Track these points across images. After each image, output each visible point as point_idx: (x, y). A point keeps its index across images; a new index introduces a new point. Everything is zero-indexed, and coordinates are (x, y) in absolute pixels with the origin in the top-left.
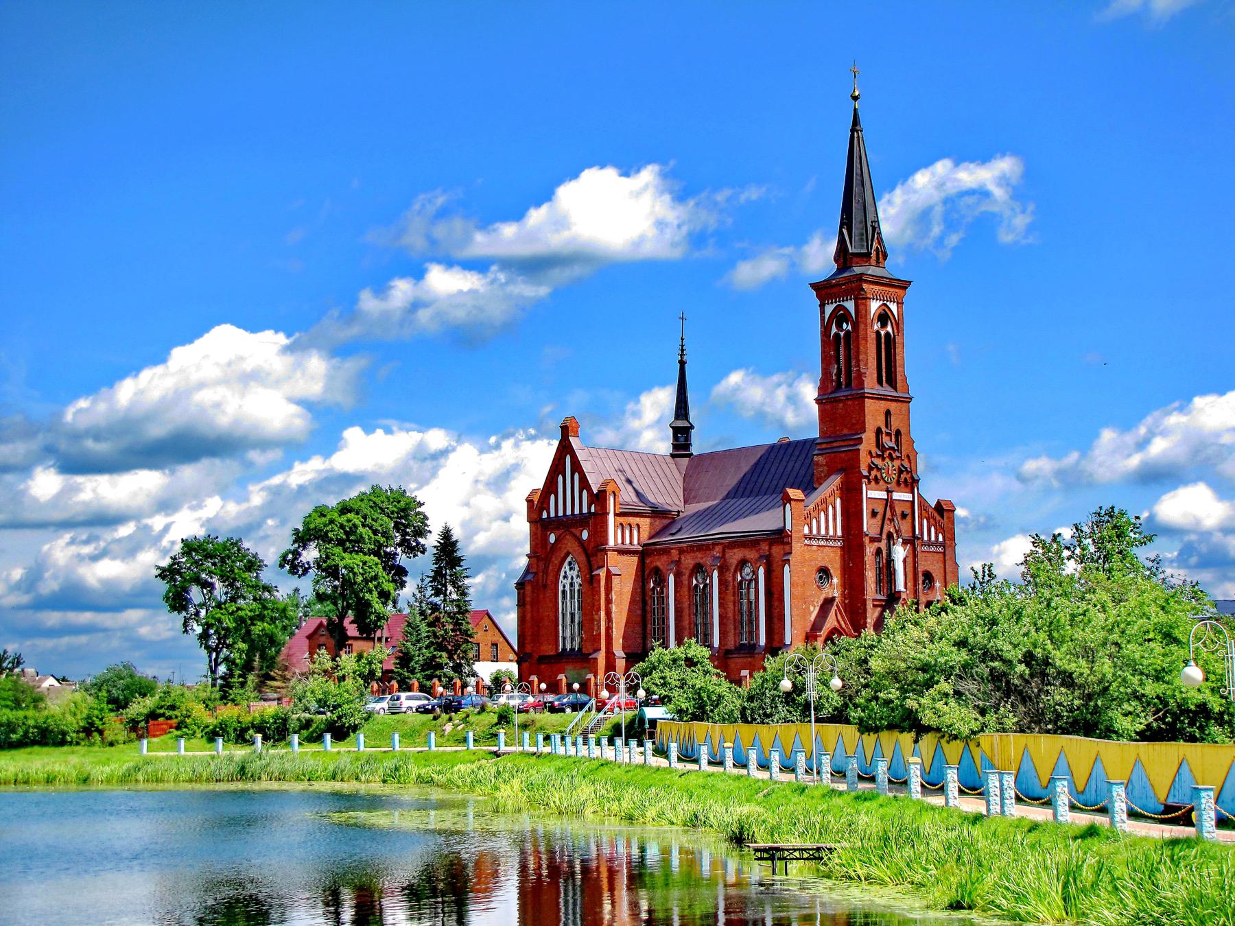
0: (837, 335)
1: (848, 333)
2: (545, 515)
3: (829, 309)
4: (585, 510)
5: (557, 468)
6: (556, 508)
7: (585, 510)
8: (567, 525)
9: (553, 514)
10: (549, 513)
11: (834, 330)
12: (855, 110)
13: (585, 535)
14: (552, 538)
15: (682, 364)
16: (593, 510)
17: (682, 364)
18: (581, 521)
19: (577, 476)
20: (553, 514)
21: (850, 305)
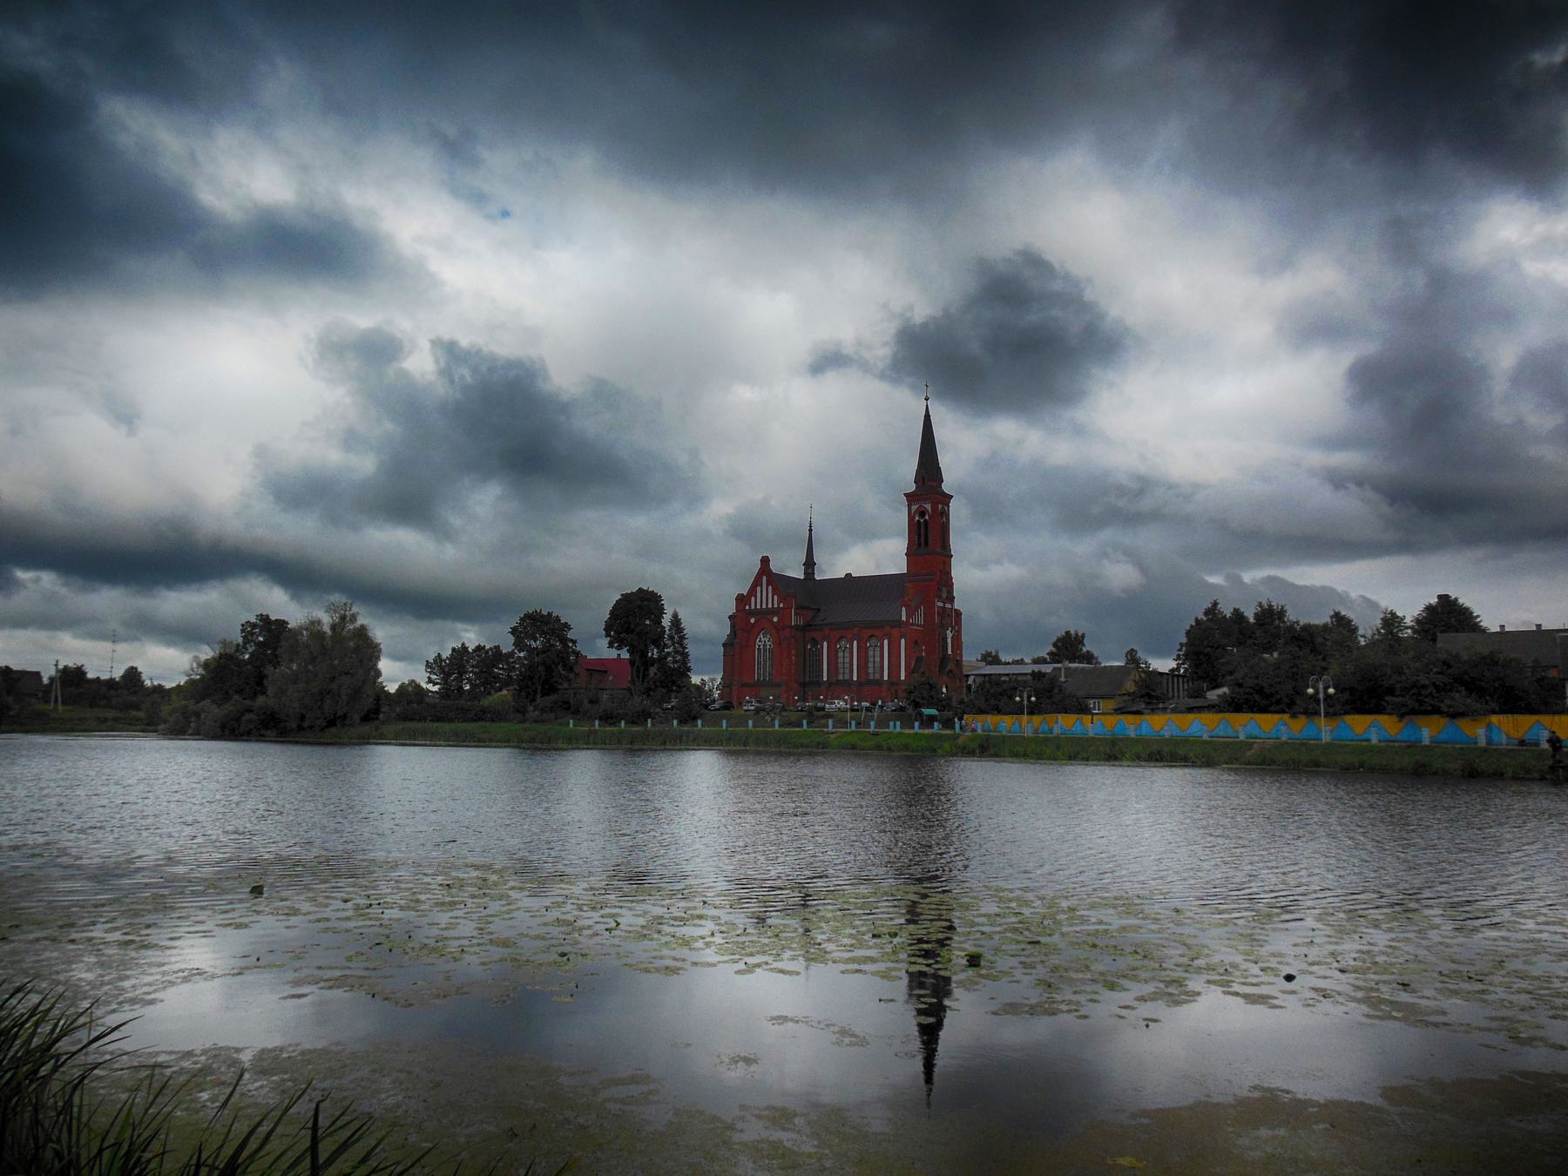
0: (918, 521)
1: (926, 520)
2: (747, 607)
3: (914, 508)
4: (776, 606)
5: (757, 582)
6: (755, 604)
7: (776, 606)
8: (763, 614)
9: (753, 607)
10: (750, 607)
11: (917, 518)
12: (927, 406)
13: (775, 619)
14: (753, 620)
15: (810, 530)
16: (781, 605)
17: (810, 530)
18: (773, 612)
19: (770, 588)
20: (753, 607)
21: (928, 507)
